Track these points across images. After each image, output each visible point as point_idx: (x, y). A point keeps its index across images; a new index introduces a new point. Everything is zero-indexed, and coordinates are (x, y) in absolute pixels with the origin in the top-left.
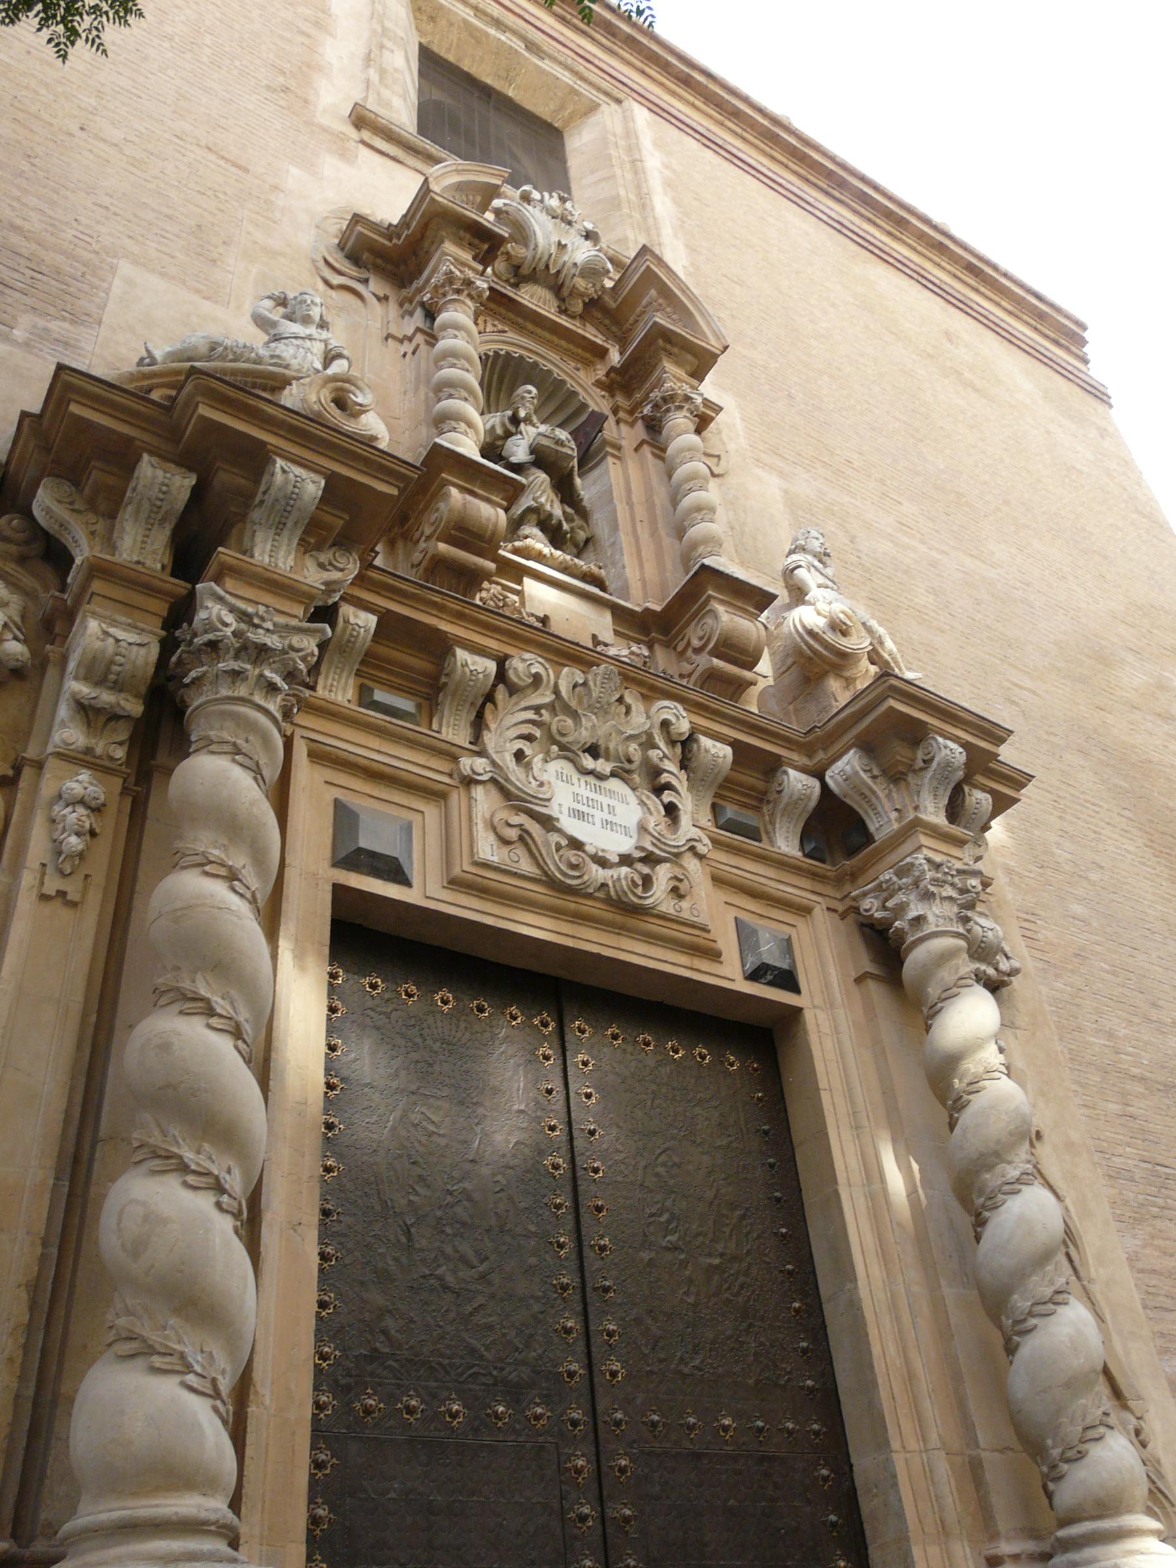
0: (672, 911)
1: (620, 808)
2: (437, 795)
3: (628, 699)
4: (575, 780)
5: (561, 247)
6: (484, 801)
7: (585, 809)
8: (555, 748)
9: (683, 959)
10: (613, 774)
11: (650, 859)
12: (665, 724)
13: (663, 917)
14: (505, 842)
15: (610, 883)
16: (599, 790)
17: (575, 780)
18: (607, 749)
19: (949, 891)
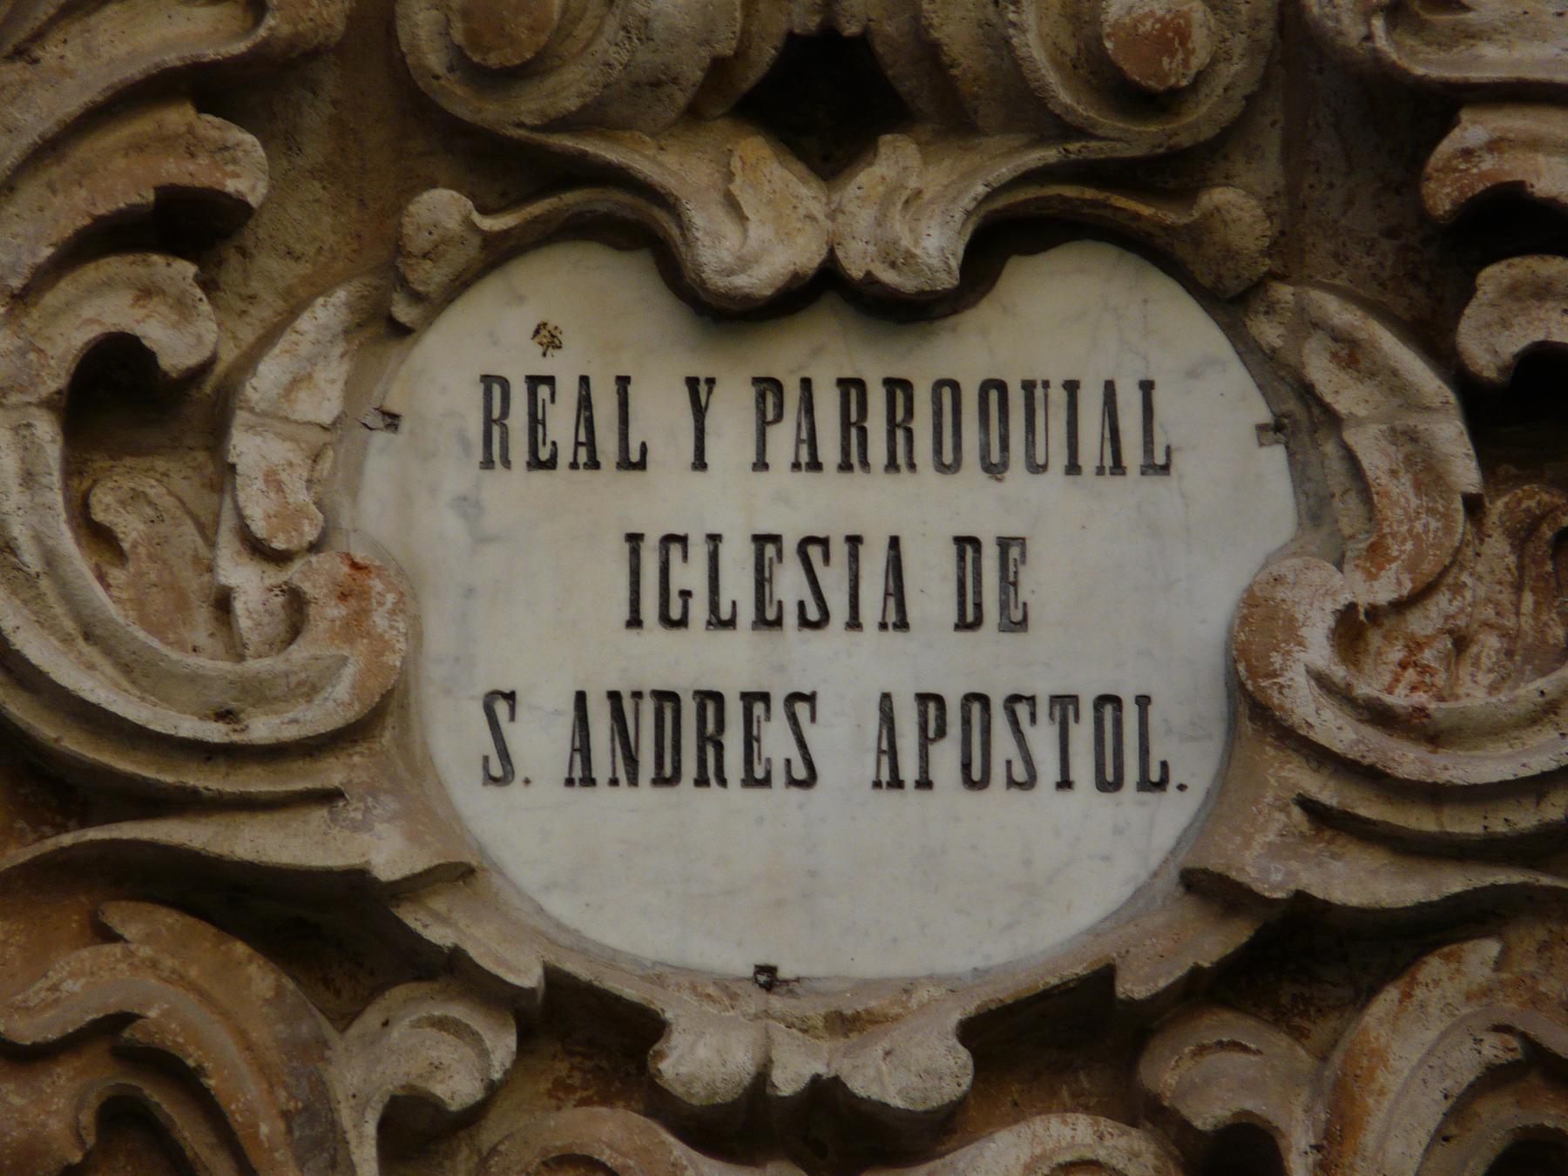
4: (661, 416)
7: (726, 661)
8: (442, 209)
10: (999, 241)
11: (1294, 963)
16: (878, 425)
17: (661, 416)
18: (931, 54)
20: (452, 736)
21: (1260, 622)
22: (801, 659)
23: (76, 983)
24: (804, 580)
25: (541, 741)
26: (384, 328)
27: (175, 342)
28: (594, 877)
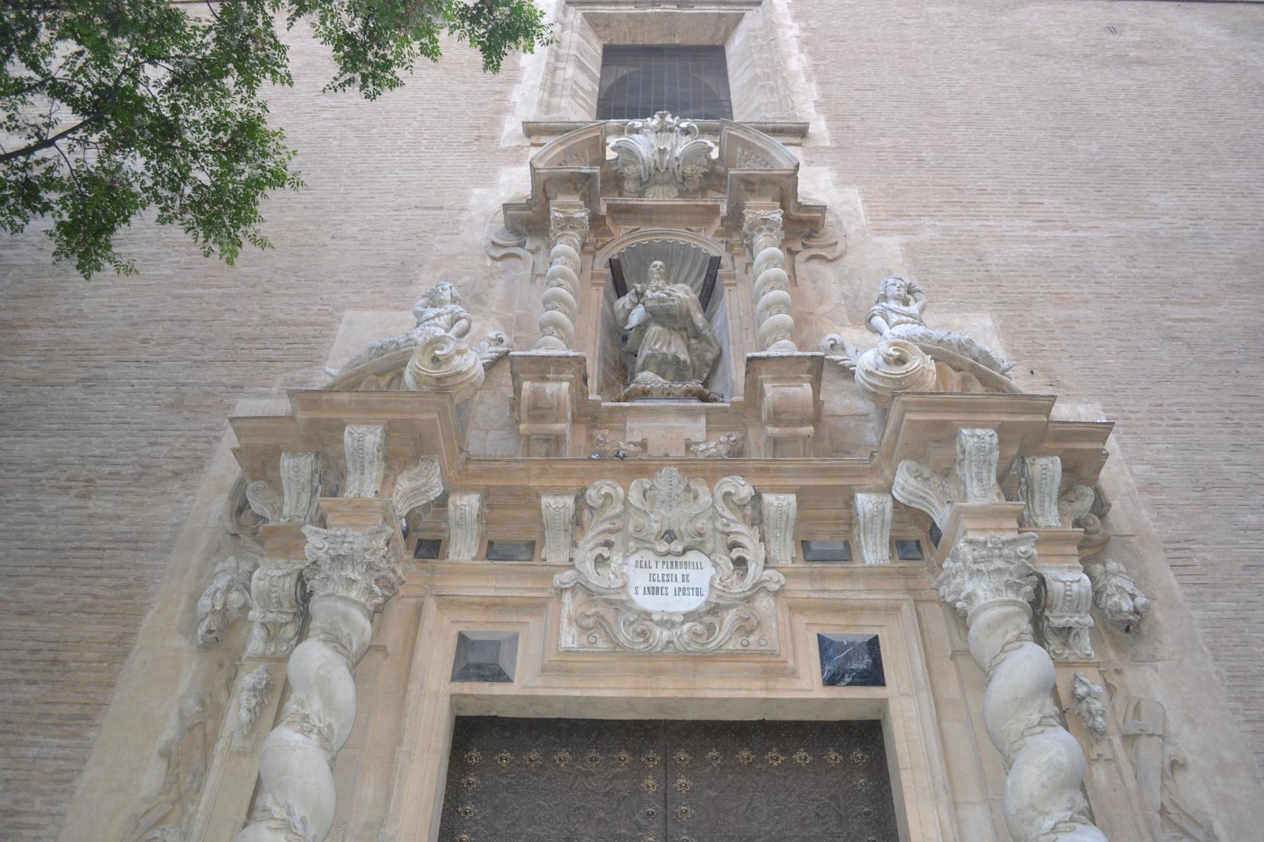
0: (739, 647)
2: (534, 607)
3: (693, 486)
4: (653, 564)
5: (662, 152)
7: (660, 584)
8: (632, 544)
10: (685, 551)
14: (584, 629)
15: (675, 639)
16: (674, 565)
19: (999, 564)
20: (632, 591)
21: (712, 579)
22: (666, 584)
25: (641, 591)
26: (626, 556)
27: (606, 555)
28: (645, 602)
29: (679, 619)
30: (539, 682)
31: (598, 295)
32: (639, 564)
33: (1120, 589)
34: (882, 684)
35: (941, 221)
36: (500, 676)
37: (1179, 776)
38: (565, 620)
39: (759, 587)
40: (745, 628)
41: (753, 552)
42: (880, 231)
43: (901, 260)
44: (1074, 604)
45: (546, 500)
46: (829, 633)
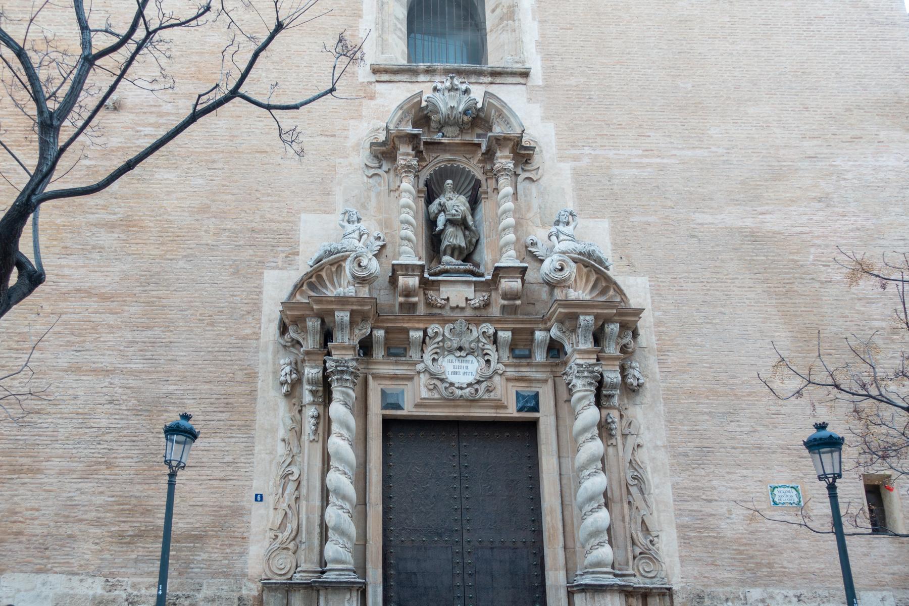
1: (469, 365)
2: (410, 378)
5: (452, 108)
6: (424, 378)
9: (493, 411)
12: (484, 332)
13: (484, 400)
14: (430, 390)
16: (462, 361)
19: (586, 374)
23: (433, 382)
24: (459, 367)
28: (452, 378)
29: (465, 386)
30: (414, 410)
31: (422, 202)
32: (449, 361)
33: (634, 376)
34: (538, 411)
35: (594, 150)
36: (399, 407)
37: (639, 450)
38: (422, 385)
39: (495, 372)
40: (488, 390)
41: (494, 357)
42: (562, 158)
43: (569, 181)
44: (613, 386)
45: (412, 333)
46: (519, 389)
